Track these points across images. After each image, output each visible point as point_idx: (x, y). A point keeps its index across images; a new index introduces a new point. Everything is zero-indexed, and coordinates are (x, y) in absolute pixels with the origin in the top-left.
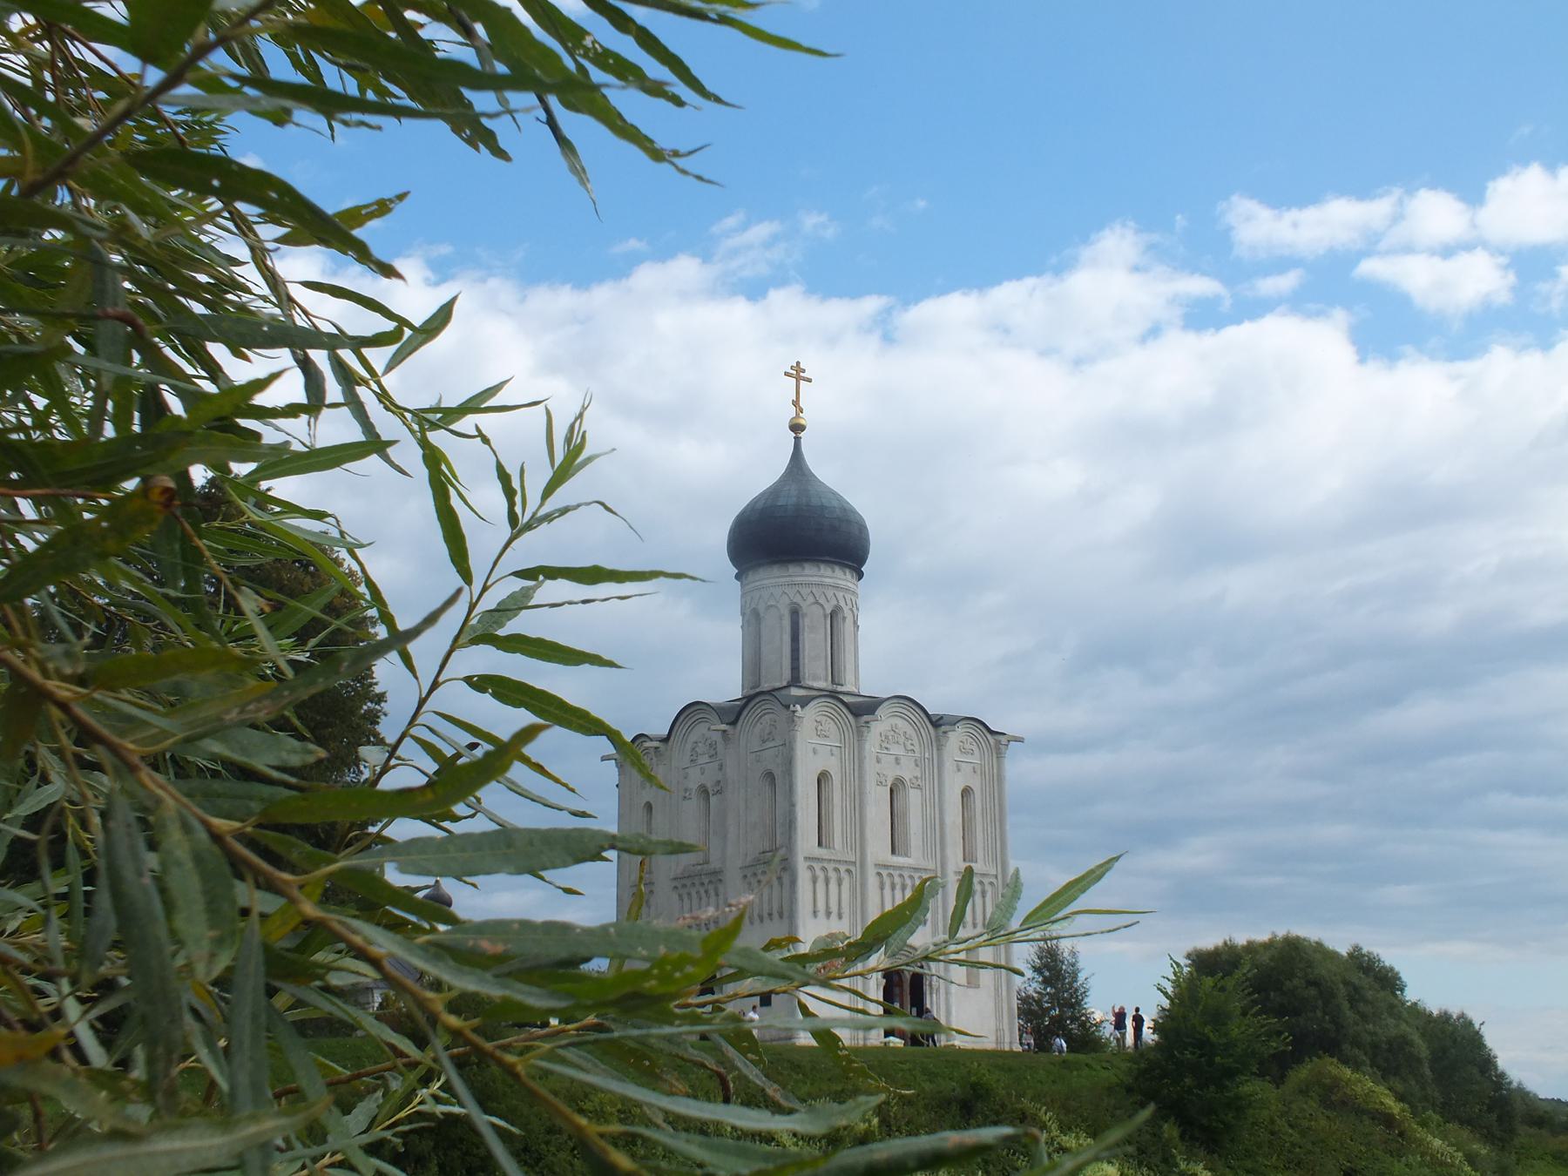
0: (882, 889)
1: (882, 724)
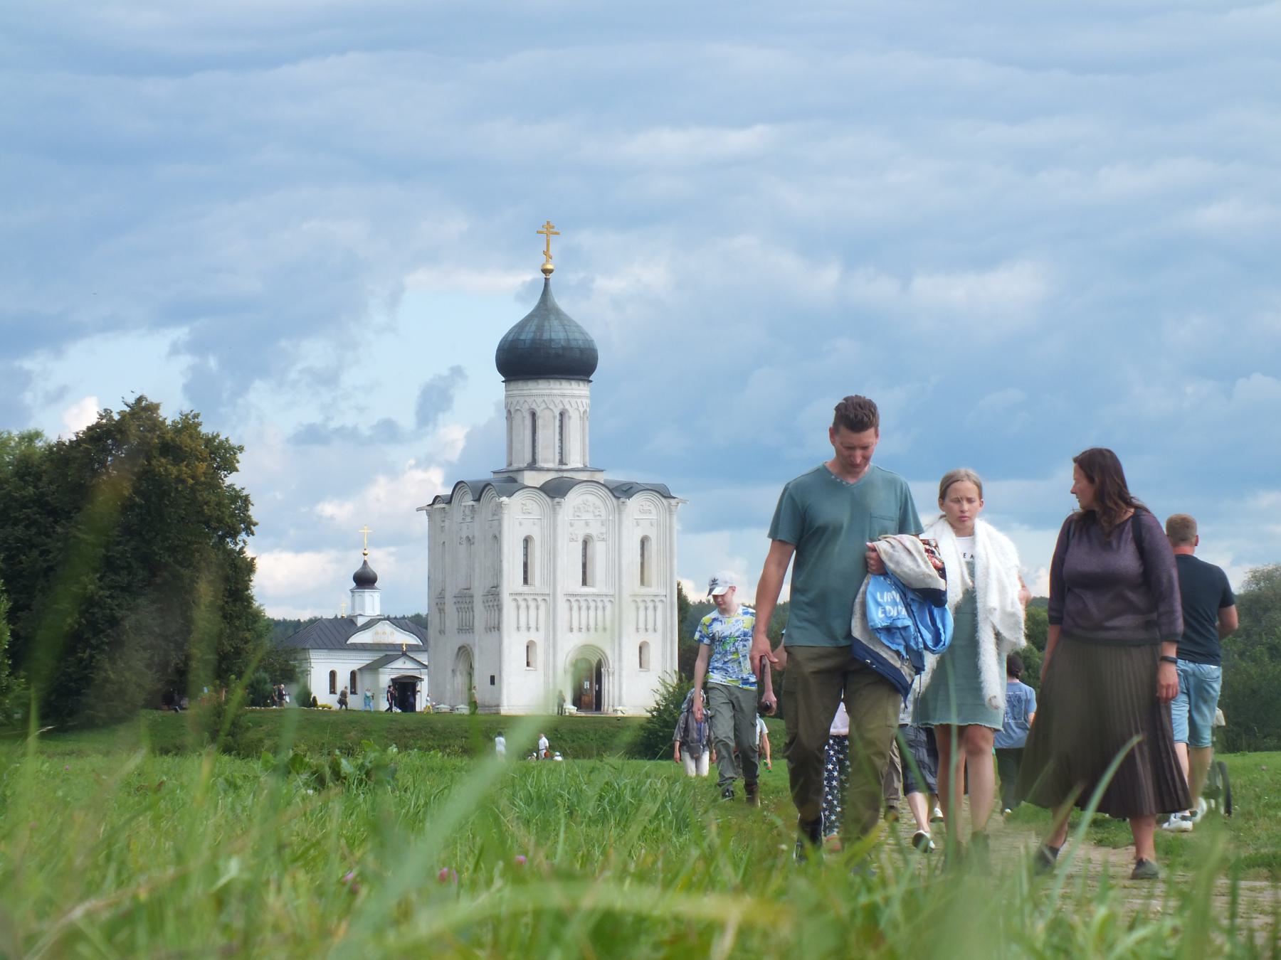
0: (571, 609)
1: (573, 499)
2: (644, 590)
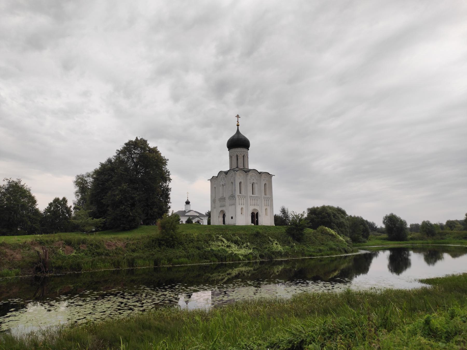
1: (250, 174)
2: (266, 196)
